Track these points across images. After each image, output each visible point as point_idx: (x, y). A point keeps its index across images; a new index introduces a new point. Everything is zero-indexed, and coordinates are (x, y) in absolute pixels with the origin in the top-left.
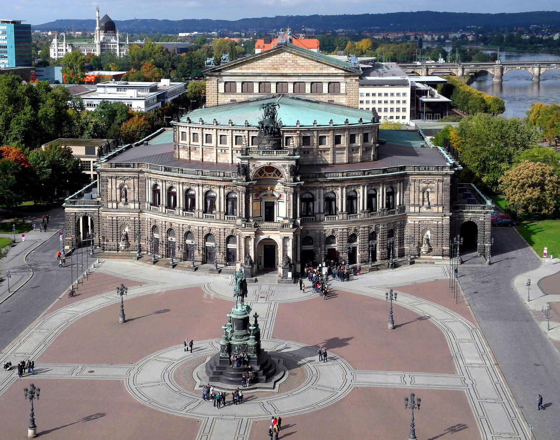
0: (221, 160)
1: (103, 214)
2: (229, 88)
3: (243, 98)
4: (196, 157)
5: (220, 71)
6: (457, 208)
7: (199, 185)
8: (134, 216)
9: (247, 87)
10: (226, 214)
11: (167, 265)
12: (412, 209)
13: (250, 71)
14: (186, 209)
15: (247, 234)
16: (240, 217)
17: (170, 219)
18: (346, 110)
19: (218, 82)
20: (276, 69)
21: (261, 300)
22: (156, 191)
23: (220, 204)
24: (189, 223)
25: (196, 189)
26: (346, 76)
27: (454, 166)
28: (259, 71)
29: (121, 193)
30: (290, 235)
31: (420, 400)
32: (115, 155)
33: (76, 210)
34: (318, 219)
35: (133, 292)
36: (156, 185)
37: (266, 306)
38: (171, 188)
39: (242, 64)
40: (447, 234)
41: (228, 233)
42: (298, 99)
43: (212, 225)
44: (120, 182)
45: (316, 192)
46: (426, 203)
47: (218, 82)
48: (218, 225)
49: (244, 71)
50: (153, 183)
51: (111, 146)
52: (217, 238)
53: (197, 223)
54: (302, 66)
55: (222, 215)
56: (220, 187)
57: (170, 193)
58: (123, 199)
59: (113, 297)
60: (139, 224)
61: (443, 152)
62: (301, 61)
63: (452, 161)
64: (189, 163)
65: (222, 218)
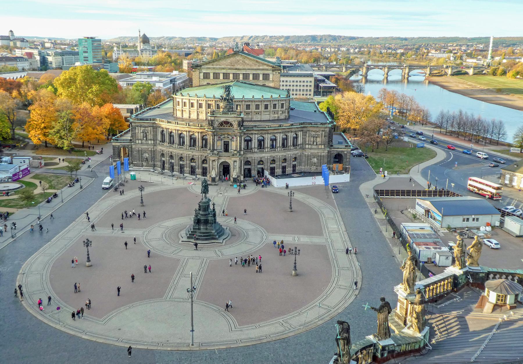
1: (134, 146)
2: (206, 76)
3: (214, 83)
8: (151, 148)
12: (307, 146)
13: (218, 66)
15: (213, 158)
16: (210, 149)
17: (171, 150)
18: (272, 90)
19: (200, 73)
20: (233, 66)
21: (220, 195)
24: (181, 152)
26: (273, 71)
27: (332, 122)
28: (223, 67)
29: (144, 135)
30: (237, 159)
31: (299, 250)
33: (119, 144)
34: (253, 151)
35: (148, 190)
36: (163, 131)
37: (222, 199)
41: (203, 158)
42: (245, 83)
43: (194, 153)
45: (253, 136)
46: (315, 143)
47: (200, 73)
49: (215, 66)
50: (161, 129)
51: (139, 109)
54: (248, 64)
55: (200, 148)
56: (198, 132)
58: (145, 139)
59: (137, 193)
60: (154, 152)
61: (326, 115)
62: (247, 61)
63: (330, 120)
64: (183, 120)
65: (200, 150)
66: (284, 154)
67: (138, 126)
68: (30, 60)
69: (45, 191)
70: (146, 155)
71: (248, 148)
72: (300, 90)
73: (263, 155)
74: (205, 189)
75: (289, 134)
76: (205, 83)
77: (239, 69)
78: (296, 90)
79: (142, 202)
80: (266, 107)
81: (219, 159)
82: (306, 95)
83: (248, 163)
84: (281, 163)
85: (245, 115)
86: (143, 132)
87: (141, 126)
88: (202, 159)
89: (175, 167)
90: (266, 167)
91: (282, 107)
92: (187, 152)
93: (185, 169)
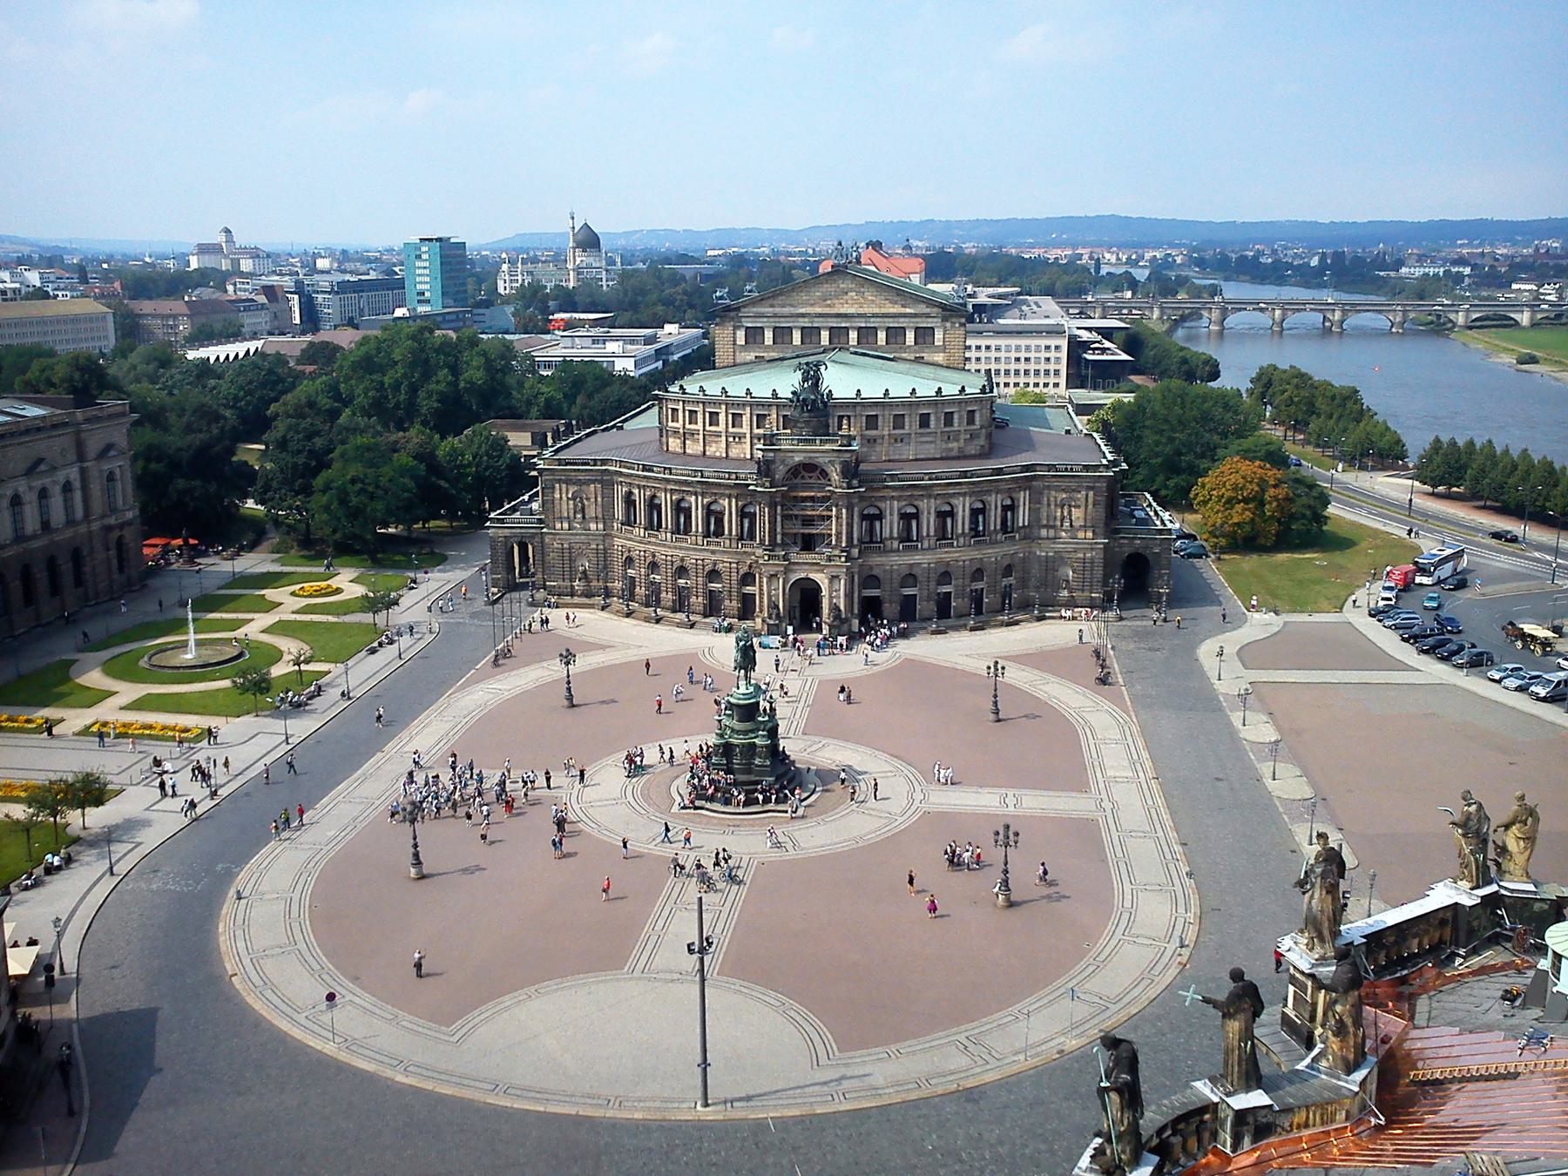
0: (734, 452)
2: (754, 335)
3: (775, 355)
4: (694, 448)
5: (738, 309)
6: (1117, 531)
7: (696, 494)
9: (782, 334)
10: (741, 538)
11: (647, 620)
12: (1044, 532)
13: (787, 310)
14: (676, 531)
22: (629, 502)
23: (731, 524)
25: (693, 499)
26: (945, 319)
27: (1114, 463)
29: (575, 506)
31: (1017, 834)
32: (567, 446)
36: (630, 493)
38: (654, 496)
39: (774, 297)
40: (1099, 573)
44: (572, 489)
47: (735, 328)
48: (723, 555)
49: (777, 310)
52: (725, 577)
53: (695, 551)
57: (653, 506)
59: (554, 670)
63: (1110, 457)
66: (976, 554)
67: (559, 481)
68: (274, 307)
69: (303, 667)
70: (585, 564)
71: (871, 542)
72: (1027, 372)
73: (917, 558)
74: (747, 659)
75: (991, 499)
76: (751, 356)
77: (845, 316)
78: (1017, 372)
79: (570, 698)
80: (924, 421)
81: (787, 571)
82: (1046, 385)
83: (871, 580)
84: (967, 581)
85: (862, 445)
86: (574, 499)
87: (568, 482)
88: (742, 572)
89: (663, 595)
90: (925, 593)
91: (971, 421)
92: (695, 551)
93: (693, 599)
